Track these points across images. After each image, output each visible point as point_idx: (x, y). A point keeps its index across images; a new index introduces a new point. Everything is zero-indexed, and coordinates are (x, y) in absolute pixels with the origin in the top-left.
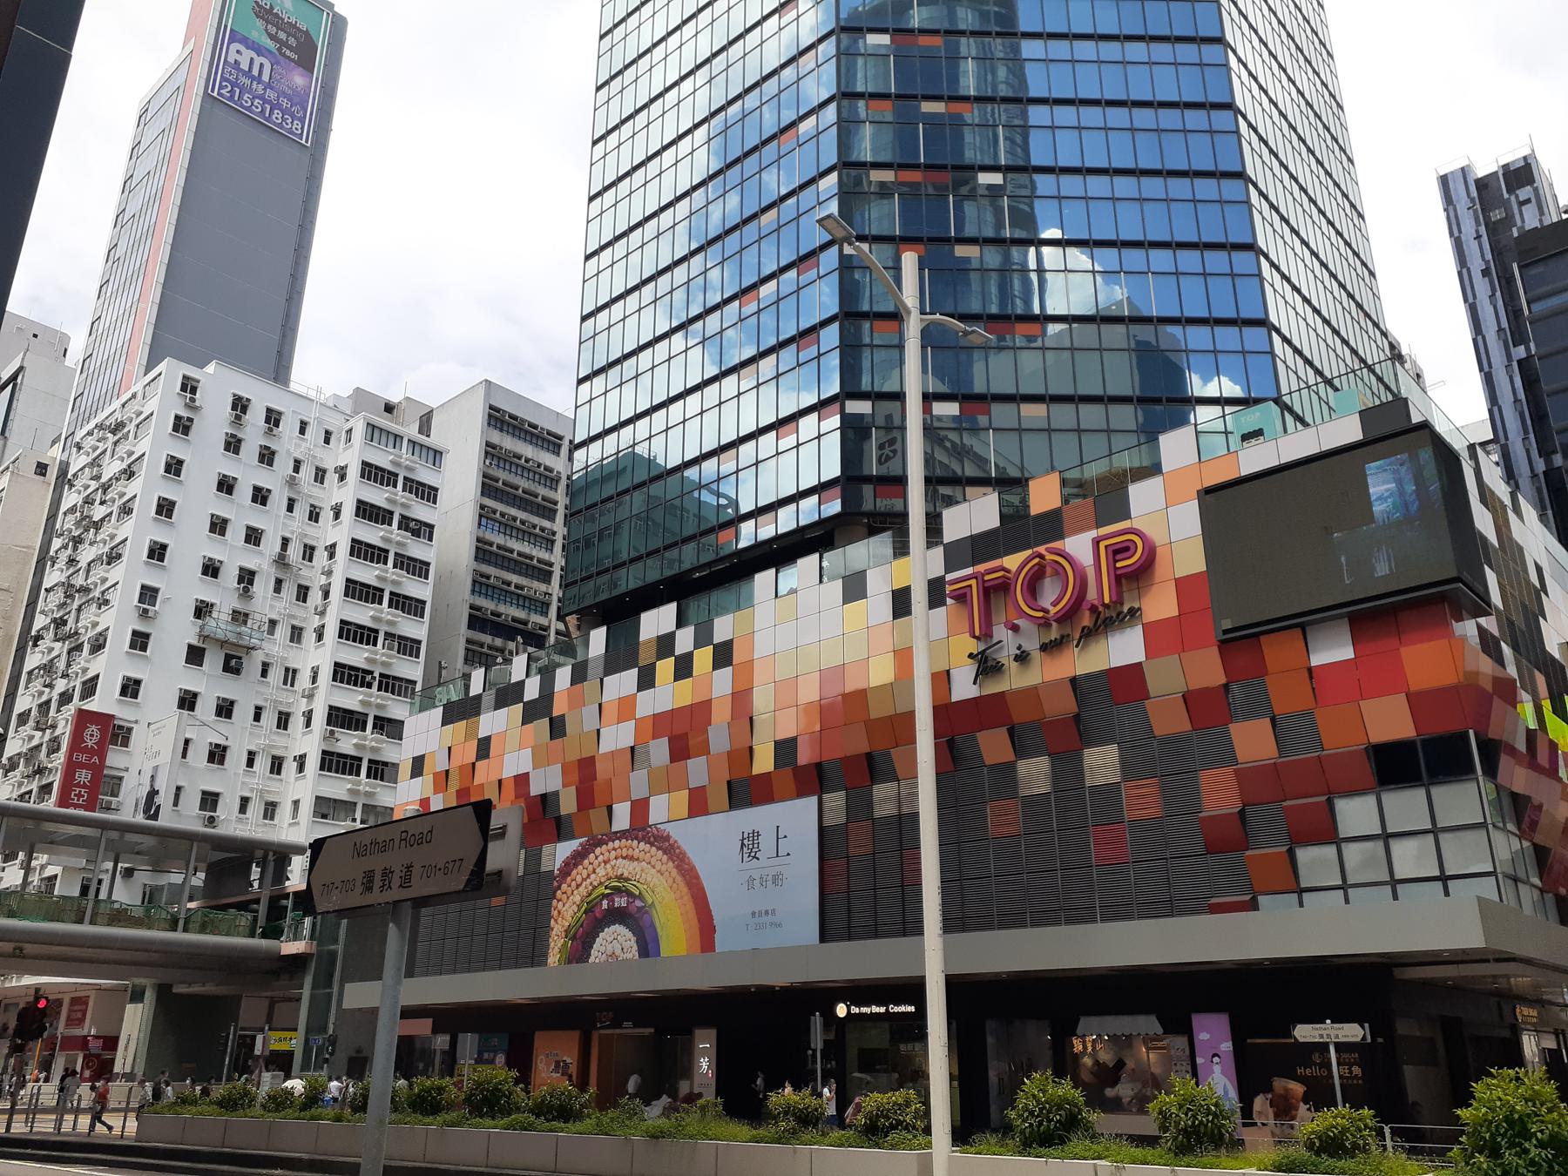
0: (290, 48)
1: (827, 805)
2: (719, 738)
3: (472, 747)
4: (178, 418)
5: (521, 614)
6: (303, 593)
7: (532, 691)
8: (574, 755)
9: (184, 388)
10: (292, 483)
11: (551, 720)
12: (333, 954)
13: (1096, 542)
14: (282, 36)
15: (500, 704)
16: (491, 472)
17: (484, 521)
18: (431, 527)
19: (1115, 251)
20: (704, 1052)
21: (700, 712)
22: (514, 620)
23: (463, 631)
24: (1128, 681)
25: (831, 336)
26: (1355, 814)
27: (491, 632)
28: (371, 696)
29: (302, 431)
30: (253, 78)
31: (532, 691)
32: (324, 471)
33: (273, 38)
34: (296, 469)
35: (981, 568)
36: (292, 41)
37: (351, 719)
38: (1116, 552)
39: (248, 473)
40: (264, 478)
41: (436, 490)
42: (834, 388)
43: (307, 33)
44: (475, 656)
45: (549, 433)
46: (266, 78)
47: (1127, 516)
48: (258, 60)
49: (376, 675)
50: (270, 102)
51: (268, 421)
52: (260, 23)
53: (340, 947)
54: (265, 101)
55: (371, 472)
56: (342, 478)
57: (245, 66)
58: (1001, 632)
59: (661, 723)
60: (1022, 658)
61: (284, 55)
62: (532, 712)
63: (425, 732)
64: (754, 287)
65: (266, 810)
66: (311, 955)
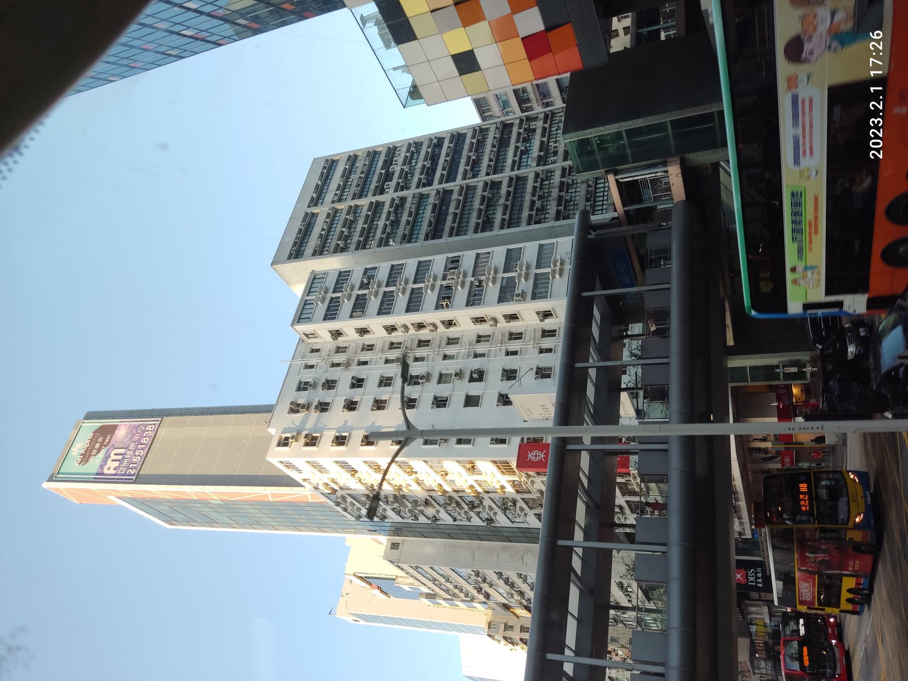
0: (104, 440)
4: (307, 444)
6: (422, 343)
9: (286, 445)
14: (97, 446)
16: (332, 249)
17: (368, 246)
23: (445, 240)
30: (124, 458)
33: (99, 451)
34: (338, 365)
36: (100, 440)
39: (344, 391)
41: (340, 273)
43: (95, 432)
46: (122, 451)
48: (113, 457)
50: (137, 446)
51: (305, 389)
52: (92, 460)
54: (137, 449)
57: (117, 464)
61: (108, 443)
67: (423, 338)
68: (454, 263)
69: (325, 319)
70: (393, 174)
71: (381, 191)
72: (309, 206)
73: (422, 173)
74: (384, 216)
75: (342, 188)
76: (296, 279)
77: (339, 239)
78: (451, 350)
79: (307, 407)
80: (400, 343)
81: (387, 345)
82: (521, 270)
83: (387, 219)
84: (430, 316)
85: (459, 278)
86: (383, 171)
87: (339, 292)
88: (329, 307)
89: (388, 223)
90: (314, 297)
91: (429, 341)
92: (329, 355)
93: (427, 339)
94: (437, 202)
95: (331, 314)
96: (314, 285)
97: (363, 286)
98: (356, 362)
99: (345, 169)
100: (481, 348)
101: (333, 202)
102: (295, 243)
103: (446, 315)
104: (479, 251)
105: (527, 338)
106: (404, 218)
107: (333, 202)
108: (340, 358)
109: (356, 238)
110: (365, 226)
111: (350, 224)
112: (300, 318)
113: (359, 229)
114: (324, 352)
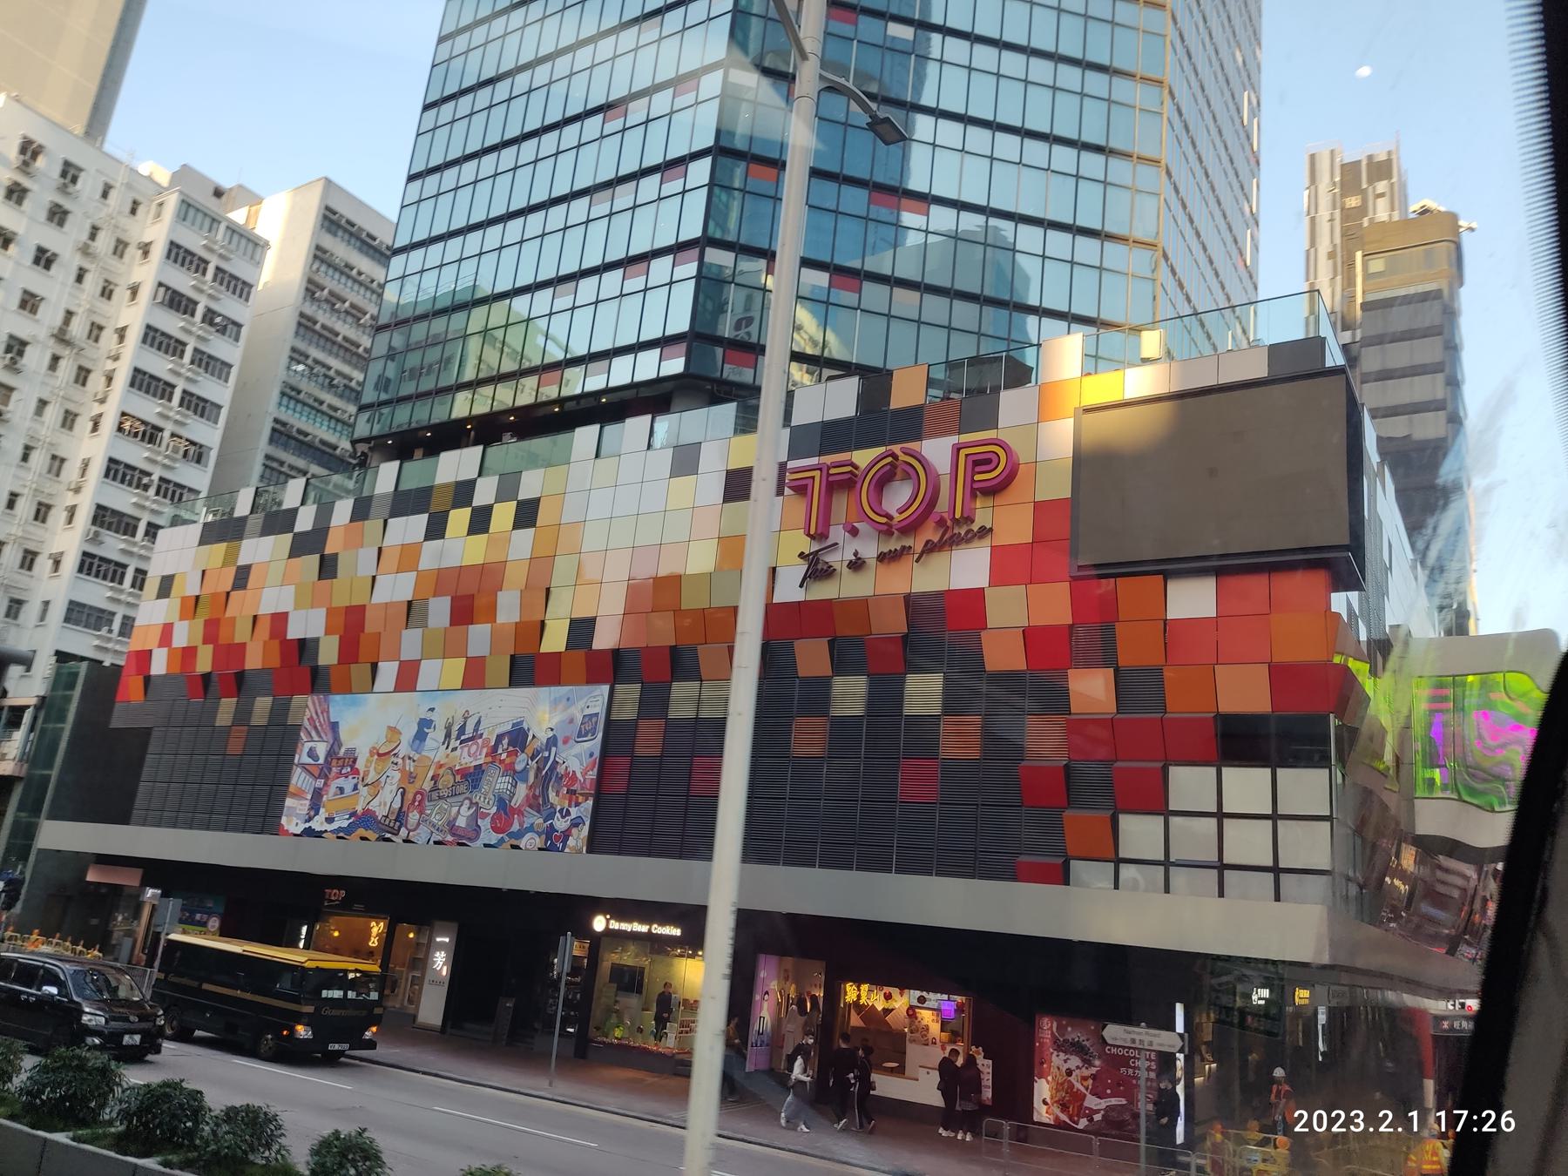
1: (618, 697)
2: (509, 608)
6: (83, 375)
7: (305, 522)
8: (342, 600)
10: (85, 251)
11: (322, 558)
12: (47, 778)
13: (957, 449)
15: (266, 531)
16: (317, 278)
18: (239, 326)
20: (441, 946)
21: (489, 576)
22: (323, 442)
23: (262, 446)
25: (700, 171)
26: (1189, 784)
28: (147, 498)
29: (105, 195)
31: (305, 522)
32: (126, 245)
34: (93, 237)
37: (119, 523)
38: (976, 463)
40: (51, 238)
42: (693, 230)
51: (64, 174)
53: (54, 773)
55: (178, 254)
56: (146, 253)
58: (837, 533)
59: (443, 580)
60: (857, 565)
62: (302, 545)
63: (179, 552)
65: (10, 608)
66: (19, 779)
67: (92, 377)
69: (172, 243)
74: (346, 369)
78: (53, 414)
79: (25, 168)
80: (96, 340)
81: (99, 320)
83: (338, 373)
84: (119, 397)
85: (166, 457)
87: (216, 275)
89: (332, 373)
91: (84, 384)
92: (116, 227)
96: (244, 241)
97: (210, 316)
98: (86, 265)
100: (39, 459)
105: (31, 529)
106: (329, 398)
108: (104, 243)
109: (323, 317)
110: (340, 339)
114: (126, 221)
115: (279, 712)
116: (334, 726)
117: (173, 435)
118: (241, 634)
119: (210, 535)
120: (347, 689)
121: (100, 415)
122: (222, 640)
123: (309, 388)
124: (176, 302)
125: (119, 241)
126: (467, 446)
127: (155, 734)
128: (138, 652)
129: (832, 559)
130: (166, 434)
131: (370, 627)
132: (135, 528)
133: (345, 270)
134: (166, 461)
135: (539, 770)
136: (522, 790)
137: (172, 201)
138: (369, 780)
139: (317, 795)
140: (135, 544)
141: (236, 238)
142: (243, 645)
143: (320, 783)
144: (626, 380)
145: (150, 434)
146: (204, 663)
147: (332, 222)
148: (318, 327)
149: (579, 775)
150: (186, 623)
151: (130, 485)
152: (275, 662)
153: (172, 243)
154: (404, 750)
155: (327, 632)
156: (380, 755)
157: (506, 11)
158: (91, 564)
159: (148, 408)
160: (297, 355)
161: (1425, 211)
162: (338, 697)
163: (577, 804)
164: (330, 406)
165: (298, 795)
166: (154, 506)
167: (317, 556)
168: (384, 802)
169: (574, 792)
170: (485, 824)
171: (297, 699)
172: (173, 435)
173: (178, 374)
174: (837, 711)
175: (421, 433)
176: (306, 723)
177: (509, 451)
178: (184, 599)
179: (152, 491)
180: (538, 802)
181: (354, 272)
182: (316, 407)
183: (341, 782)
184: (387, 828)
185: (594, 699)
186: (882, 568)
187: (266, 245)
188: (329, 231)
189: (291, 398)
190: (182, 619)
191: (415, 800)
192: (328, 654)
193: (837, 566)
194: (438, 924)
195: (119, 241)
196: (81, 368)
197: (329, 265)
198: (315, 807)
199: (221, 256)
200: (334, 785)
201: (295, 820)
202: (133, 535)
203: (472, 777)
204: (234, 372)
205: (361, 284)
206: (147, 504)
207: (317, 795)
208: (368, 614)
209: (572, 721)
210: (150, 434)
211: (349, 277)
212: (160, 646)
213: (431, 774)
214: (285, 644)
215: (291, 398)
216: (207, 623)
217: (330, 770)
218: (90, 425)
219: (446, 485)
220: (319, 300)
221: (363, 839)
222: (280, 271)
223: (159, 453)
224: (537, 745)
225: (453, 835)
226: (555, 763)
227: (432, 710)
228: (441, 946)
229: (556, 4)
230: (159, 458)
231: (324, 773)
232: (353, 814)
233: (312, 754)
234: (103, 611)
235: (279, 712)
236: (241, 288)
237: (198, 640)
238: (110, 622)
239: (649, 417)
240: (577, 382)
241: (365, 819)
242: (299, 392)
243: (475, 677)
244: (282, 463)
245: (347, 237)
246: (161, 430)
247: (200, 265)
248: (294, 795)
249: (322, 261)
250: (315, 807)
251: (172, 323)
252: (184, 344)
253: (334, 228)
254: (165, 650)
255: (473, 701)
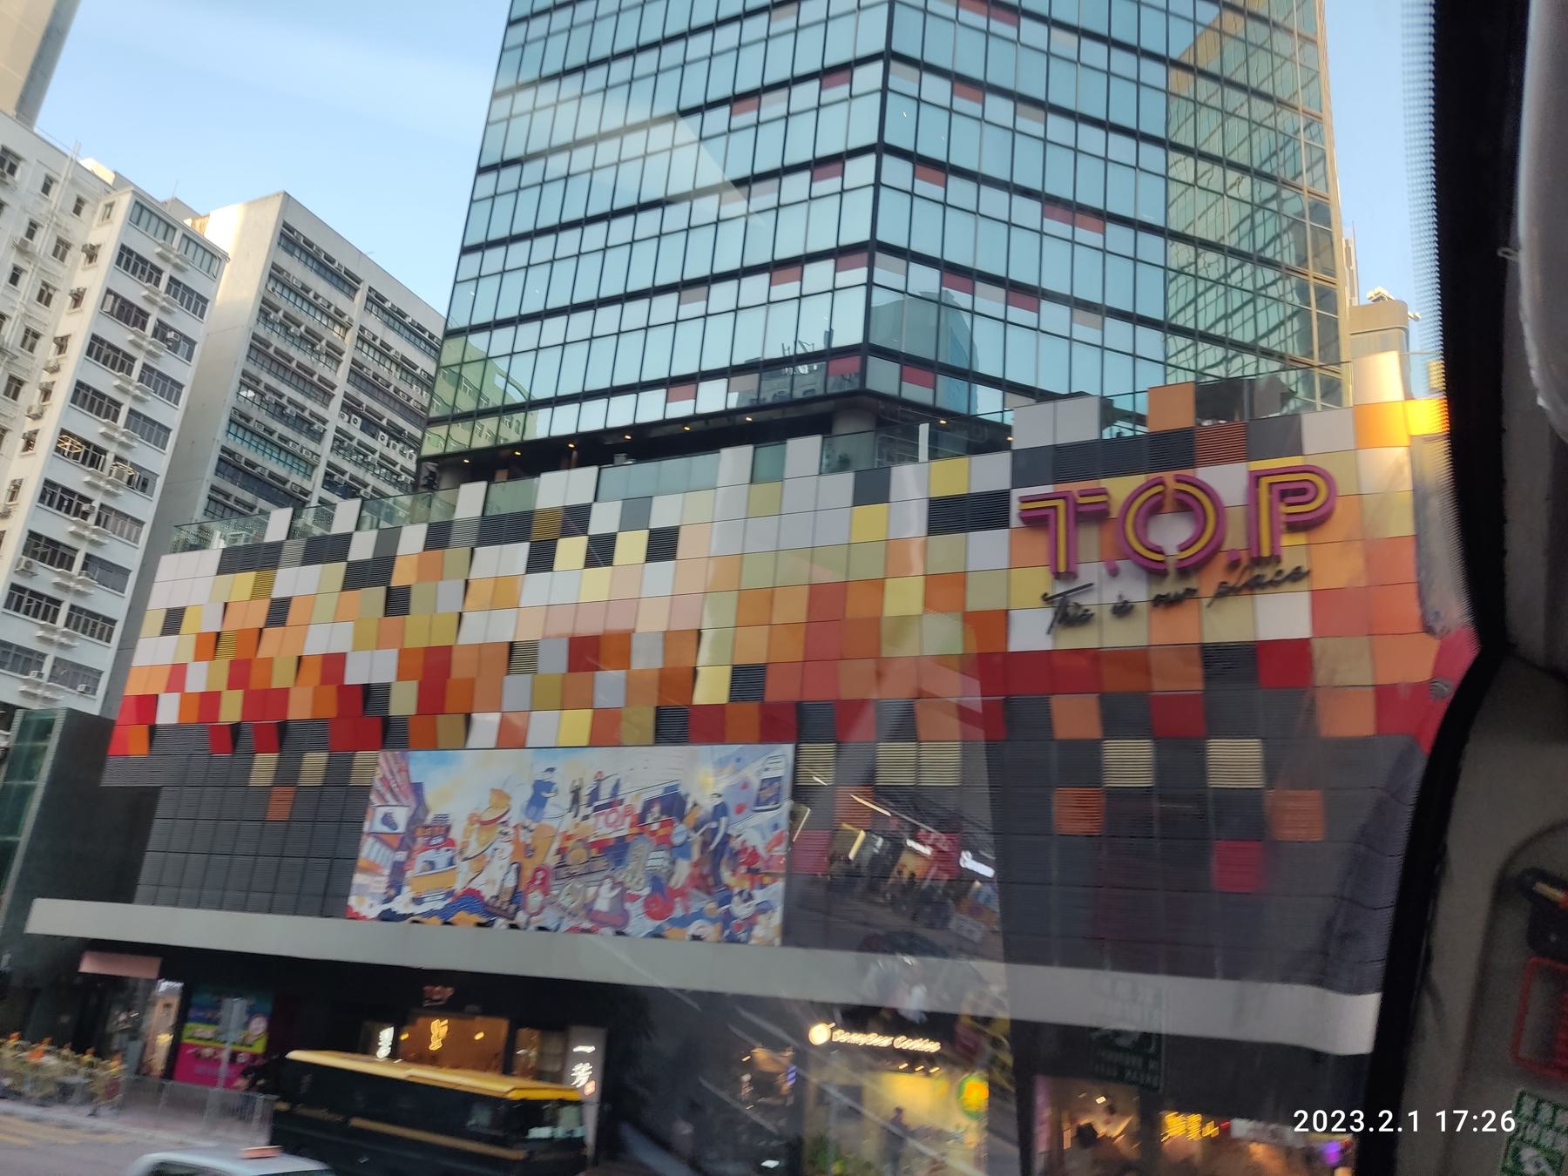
1: (804, 758)
3: (261, 609)
5: (280, 471)
11: (389, 591)
13: (1256, 478)
16: (272, 299)
17: (254, 354)
18: (192, 343)
19: (914, 248)
20: (583, 1058)
22: (272, 475)
24: (1291, 658)
27: (244, 483)
29: (46, 189)
32: (68, 246)
34: (31, 234)
35: (1074, 487)
37: (54, 553)
38: (1284, 494)
41: (206, 301)
44: (219, 505)
45: (347, 272)
47: (1298, 450)
49: (96, 504)
53: (23, 839)
58: (1090, 571)
60: (1123, 610)
62: (358, 577)
63: (193, 581)
64: (756, 94)
67: (24, 390)
68: (142, 483)
69: (123, 247)
70: (373, 436)
71: (350, 407)
72: (371, 289)
73: (352, 478)
74: (299, 398)
75: (383, 351)
76: (235, 231)
77: (286, 316)
80: (31, 349)
82: (80, 582)
83: (290, 401)
84: (58, 413)
85: (109, 482)
86: (384, 422)
88: (145, 261)
89: (284, 401)
90: (175, 244)
91: (15, 397)
93: (21, 396)
94: (288, 486)
95: (128, 261)
96: (200, 251)
97: (161, 330)
98: (22, 264)
99: (415, 367)
101: (362, 329)
102: (311, 245)
103: (45, 442)
104: (146, 530)
106: (280, 428)
107: (362, 329)
109: (277, 342)
110: (294, 365)
111: (309, 340)
112: (142, 207)
113: (292, 352)
114: (69, 221)
115: (338, 772)
116: (417, 789)
117: (117, 458)
118: (282, 677)
119: (231, 562)
120: (431, 744)
121: (35, 432)
122: (256, 683)
123: (259, 415)
124: (127, 313)
125: (60, 241)
126: (569, 467)
127: (164, 795)
128: (139, 698)
129: (1087, 601)
130: (110, 457)
131: (459, 671)
132: (72, 560)
133: (301, 293)
134: (109, 487)
135: (705, 845)
136: (683, 869)
137: (124, 203)
138: (470, 852)
139: (398, 870)
140: (71, 578)
141: (192, 247)
142: (285, 692)
143: (401, 856)
144: (628, 421)
145: (91, 456)
146: (231, 710)
147: (288, 239)
148: (271, 351)
149: (761, 851)
150: (204, 664)
151: (67, 512)
152: (330, 710)
153: (123, 247)
154: (515, 817)
155: (401, 676)
156: (484, 823)
157: (547, 11)
158: (20, 599)
159: (91, 428)
160: (248, 381)
161: (1380, 298)
162: (420, 754)
163: (763, 886)
164: (281, 438)
165: (372, 869)
166: (94, 537)
167: (381, 591)
168: (493, 881)
169: (757, 872)
170: (635, 908)
171: (362, 757)
172: (117, 458)
173: (125, 392)
174: (1113, 781)
175: (738, 418)
176: (378, 784)
177: (628, 475)
178: (200, 636)
179: (91, 520)
180: (707, 881)
181: (311, 295)
182: (264, 438)
183: (430, 855)
184: (484, 911)
185: (778, 760)
186: (1160, 615)
187: (226, 257)
188: (286, 249)
189: (239, 425)
190: (197, 659)
191: (535, 876)
192: (403, 702)
193: (1093, 610)
194: (575, 1030)
195: (60, 241)
196: (12, 378)
197: (284, 286)
198: (396, 885)
199: (176, 266)
200: (421, 859)
201: (368, 901)
202: (69, 568)
203: (615, 851)
204: (185, 393)
205: (317, 308)
206: (87, 533)
207: (398, 870)
208: (456, 656)
209: (745, 786)
210: (91, 456)
211: (304, 299)
212: (169, 689)
213: (555, 846)
214: (345, 691)
215: (239, 425)
216: (234, 665)
217: (414, 840)
218: (22, 442)
219: (552, 511)
220: (273, 323)
221: (696, 938)
222: (237, 290)
223: (101, 478)
224: (700, 814)
225: (592, 920)
226: (727, 837)
227: (551, 770)
228: (583, 1058)
229: (609, 3)
230: (102, 483)
231: (406, 843)
232: (450, 894)
233: (387, 820)
234: (31, 652)
235: (338, 772)
236: (197, 303)
237: (221, 684)
238: (40, 665)
239: (595, 469)
240: (542, 426)
241: (470, 899)
242: (248, 420)
243: (605, 733)
244: (227, 496)
245: (303, 257)
246: (105, 452)
247: (153, 274)
248: (365, 870)
249: (277, 281)
250: (396, 885)
251: (119, 335)
252: (133, 359)
253: (290, 247)
254: (176, 696)
255: (603, 760)
